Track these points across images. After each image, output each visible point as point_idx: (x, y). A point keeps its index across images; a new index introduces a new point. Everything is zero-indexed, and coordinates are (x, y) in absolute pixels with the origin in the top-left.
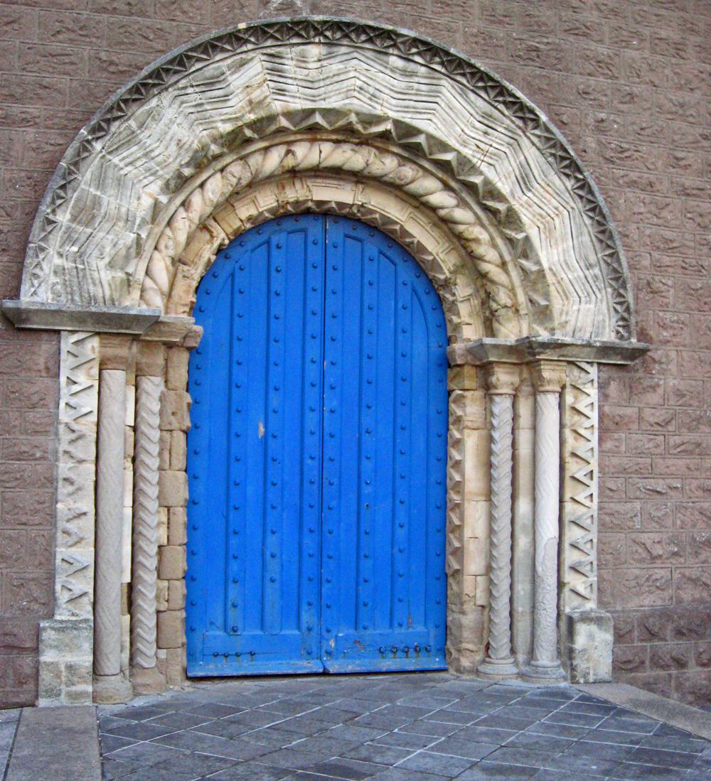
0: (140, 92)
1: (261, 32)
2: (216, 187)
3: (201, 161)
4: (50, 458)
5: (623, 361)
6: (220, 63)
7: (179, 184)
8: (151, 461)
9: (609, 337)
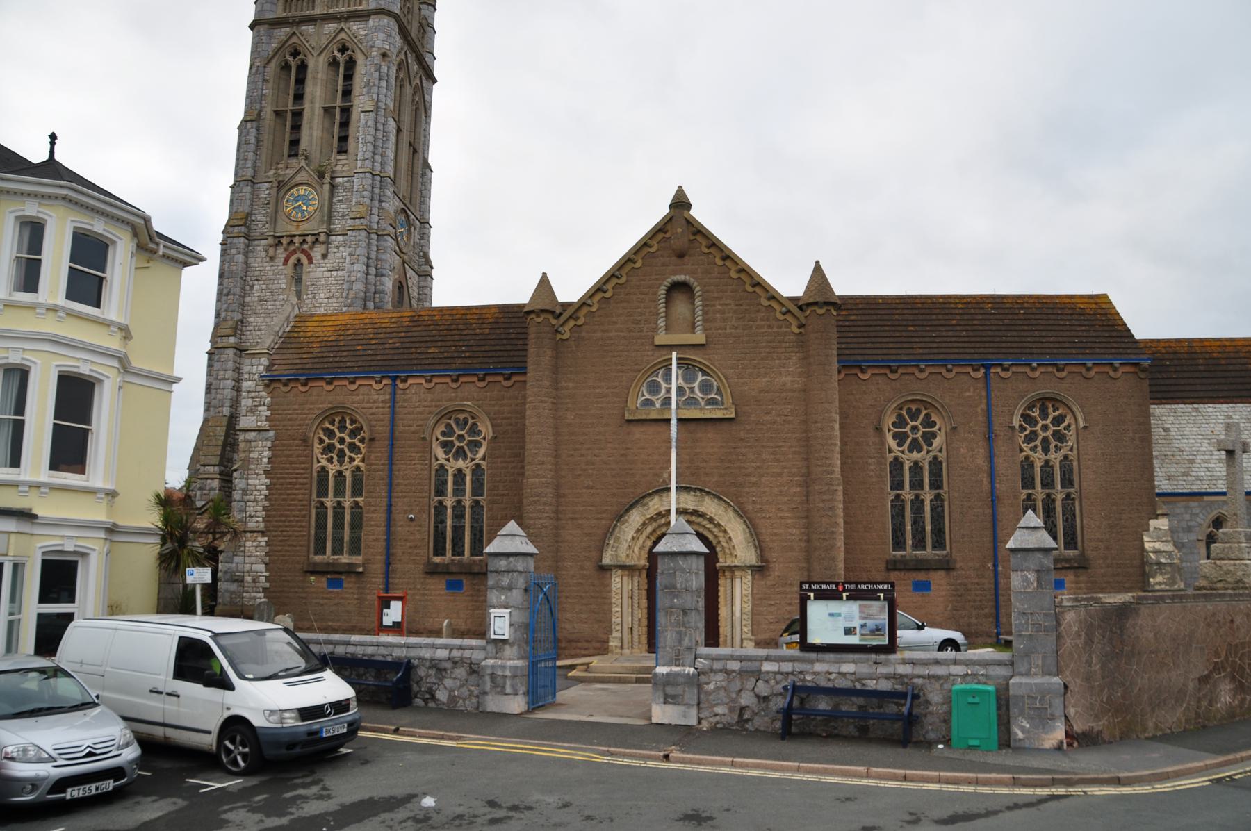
0: (628, 510)
1: (656, 492)
2: (649, 529)
3: (644, 524)
4: (610, 598)
5: (759, 570)
6: (647, 500)
7: (638, 530)
8: (636, 598)
9: (754, 562)
